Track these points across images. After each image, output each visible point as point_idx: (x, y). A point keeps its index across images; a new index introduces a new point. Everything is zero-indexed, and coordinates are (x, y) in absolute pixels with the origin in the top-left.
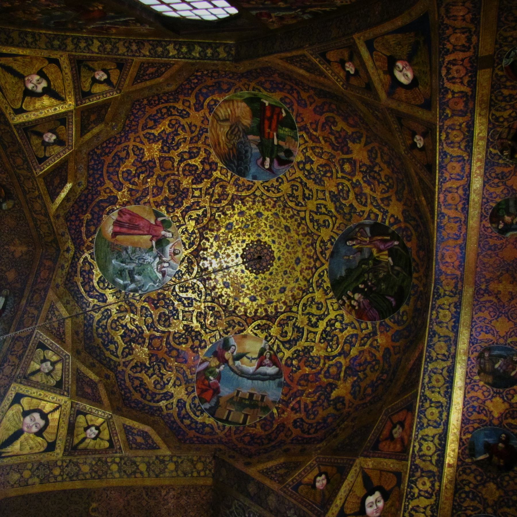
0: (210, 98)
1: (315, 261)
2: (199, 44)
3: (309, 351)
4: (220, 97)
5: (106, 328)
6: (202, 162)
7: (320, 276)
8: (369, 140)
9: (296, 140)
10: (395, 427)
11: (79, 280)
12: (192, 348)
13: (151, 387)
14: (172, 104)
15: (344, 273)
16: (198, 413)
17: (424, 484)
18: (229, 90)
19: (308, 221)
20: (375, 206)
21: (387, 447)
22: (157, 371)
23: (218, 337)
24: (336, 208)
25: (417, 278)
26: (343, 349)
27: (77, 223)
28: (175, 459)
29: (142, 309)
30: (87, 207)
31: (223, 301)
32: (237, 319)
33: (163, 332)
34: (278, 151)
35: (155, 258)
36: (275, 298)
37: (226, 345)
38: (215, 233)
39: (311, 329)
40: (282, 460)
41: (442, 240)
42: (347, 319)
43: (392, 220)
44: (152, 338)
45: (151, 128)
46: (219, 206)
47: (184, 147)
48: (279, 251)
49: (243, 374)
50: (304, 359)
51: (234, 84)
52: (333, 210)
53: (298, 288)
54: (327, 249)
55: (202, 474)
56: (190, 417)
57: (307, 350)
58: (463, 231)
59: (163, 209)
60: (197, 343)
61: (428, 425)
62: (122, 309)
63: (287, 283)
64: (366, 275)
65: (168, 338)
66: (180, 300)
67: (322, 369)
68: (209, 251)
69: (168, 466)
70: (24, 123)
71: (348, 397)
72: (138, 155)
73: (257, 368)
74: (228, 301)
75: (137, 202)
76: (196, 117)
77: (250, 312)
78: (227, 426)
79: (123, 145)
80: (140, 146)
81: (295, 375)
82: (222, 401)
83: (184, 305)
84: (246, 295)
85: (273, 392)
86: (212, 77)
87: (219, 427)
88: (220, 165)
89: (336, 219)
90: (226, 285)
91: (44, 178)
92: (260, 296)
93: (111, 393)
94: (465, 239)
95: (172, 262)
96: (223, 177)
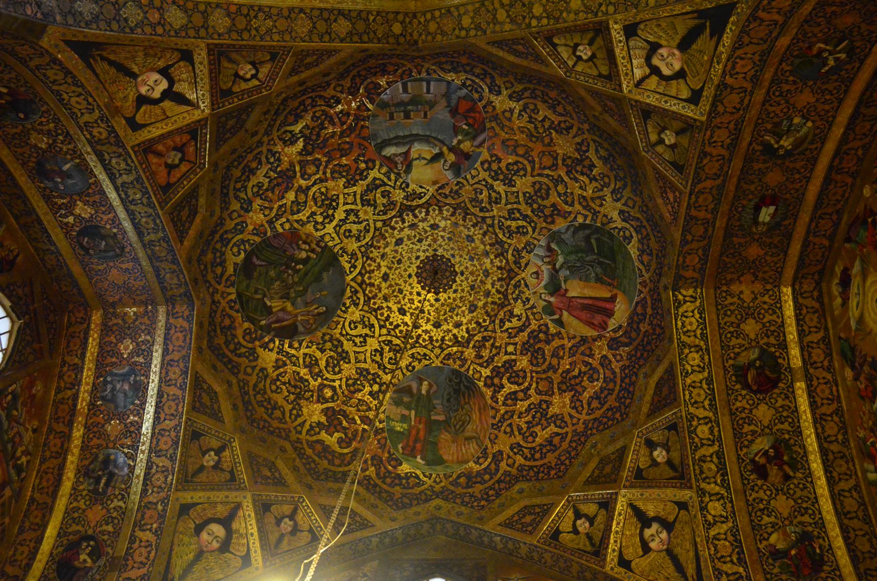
0: (483, 467)
1: (363, 281)
2: (472, 543)
3: (348, 182)
4: (471, 468)
5: (615, 177)
6: (502, 387)
7: (355, 267)
8: (299, 428)
9: (388, 417)
10: (181, 160)
11: (653, 244)
12: (499, 160)
13: (540, 105)
14: (528, 463)
15: (325, 275)
16: (468, 83)
17: (100, 133)
18: (459, 477)
19: (377, 326)
20: (294, 356)
21: (178, 139)
22: (539, 125)
23: (469, 177)
24: (342, 346)
25: (229, 294)
26: (306, 195)
27: (655, 322)
28: (463, 33)
29: (573, 202)
30: (643, 340)
31: (471, 220)
32: (449, 200)
33: (539, 175)
34: (410, 403)
35: (562, 267)
36: (407, 231)
37: (456, 169)
38: (490, 300)
39: (353, 207)
40: (322, 66)
41: (184, 357)
42: (310, 227)
43: (271, 345)
44: (554, 167)
45: (557, 434)
46: (485, 334)
47: (522, 406)
48: (410, 284)
49: (425, 139)
50: (352, 172)
51: (451, 483)
52: (345, 342)
53: (379, 248)
54: (351, 297)
55: (429, 16)
56: (478, 76)
57: (349, 184)
58: (164, 371)
59: (553, 329)
60: (494, 166)
61: (132, 183)
62: (598, 202)
63: (396, 252)
64: (296, 280)
65: (533, 169)
66: (525, 217)
67: (326, 167)
68: (495, 278)
69: (470, 21)
70: (680, 488)
71: (279, 148)
72: (578, 400)
73: (409, 149)
74: (464, 220)
75: (584, 340)
76: (503, 444)
77: (434, 212)
78: (424, 75)
79: (592, 417)
80: (573, 412)
81: (359, 151)
82: (443, 102)
83: (519, 210)
84: (444, 230)
85: (381, 127)
86: (471, 496)
87: (435, 71)
88: (481, 384)
89: (341, 334)
90: (470, 239)
91: (675, 400)
92: (426, 232)
93: (582, 99)
94: (163, 360)
95: (540, 263)
96: (479, 368)
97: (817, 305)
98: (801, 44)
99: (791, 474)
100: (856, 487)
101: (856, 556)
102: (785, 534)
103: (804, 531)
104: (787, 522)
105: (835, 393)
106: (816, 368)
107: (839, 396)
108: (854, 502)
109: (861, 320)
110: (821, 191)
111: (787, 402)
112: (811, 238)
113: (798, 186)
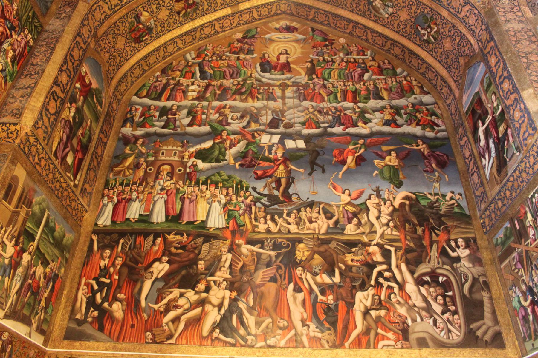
97: (272, 13)
98: (440, 20)
99: (181, 15)
100: (179, 49)
101: (147, 57)
102: (150, 19)
103: (152, 28)
104: (155, 19)
105: (226, 29)
106: (239, 17)
107: (224, 31)
108: (172, 50)
109: (271, 41)
110: (344, 17)
111: (219, 5)
112: (313, 10)
113: (348, 5)
